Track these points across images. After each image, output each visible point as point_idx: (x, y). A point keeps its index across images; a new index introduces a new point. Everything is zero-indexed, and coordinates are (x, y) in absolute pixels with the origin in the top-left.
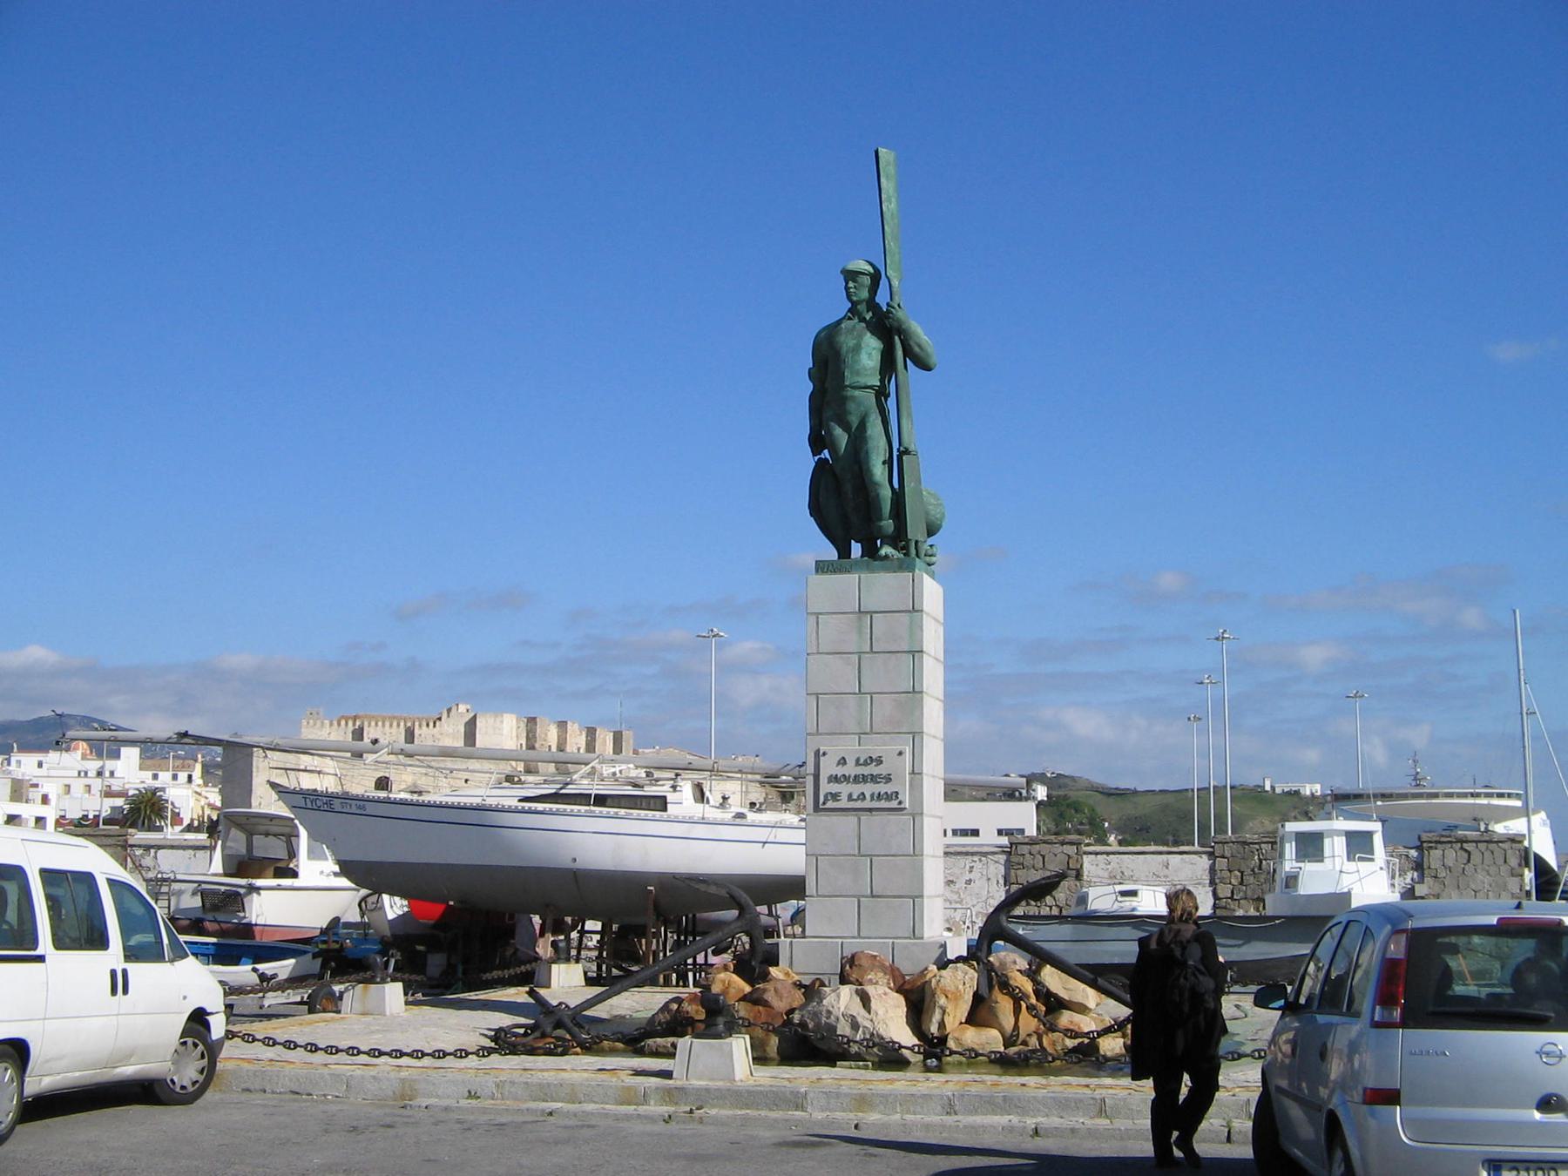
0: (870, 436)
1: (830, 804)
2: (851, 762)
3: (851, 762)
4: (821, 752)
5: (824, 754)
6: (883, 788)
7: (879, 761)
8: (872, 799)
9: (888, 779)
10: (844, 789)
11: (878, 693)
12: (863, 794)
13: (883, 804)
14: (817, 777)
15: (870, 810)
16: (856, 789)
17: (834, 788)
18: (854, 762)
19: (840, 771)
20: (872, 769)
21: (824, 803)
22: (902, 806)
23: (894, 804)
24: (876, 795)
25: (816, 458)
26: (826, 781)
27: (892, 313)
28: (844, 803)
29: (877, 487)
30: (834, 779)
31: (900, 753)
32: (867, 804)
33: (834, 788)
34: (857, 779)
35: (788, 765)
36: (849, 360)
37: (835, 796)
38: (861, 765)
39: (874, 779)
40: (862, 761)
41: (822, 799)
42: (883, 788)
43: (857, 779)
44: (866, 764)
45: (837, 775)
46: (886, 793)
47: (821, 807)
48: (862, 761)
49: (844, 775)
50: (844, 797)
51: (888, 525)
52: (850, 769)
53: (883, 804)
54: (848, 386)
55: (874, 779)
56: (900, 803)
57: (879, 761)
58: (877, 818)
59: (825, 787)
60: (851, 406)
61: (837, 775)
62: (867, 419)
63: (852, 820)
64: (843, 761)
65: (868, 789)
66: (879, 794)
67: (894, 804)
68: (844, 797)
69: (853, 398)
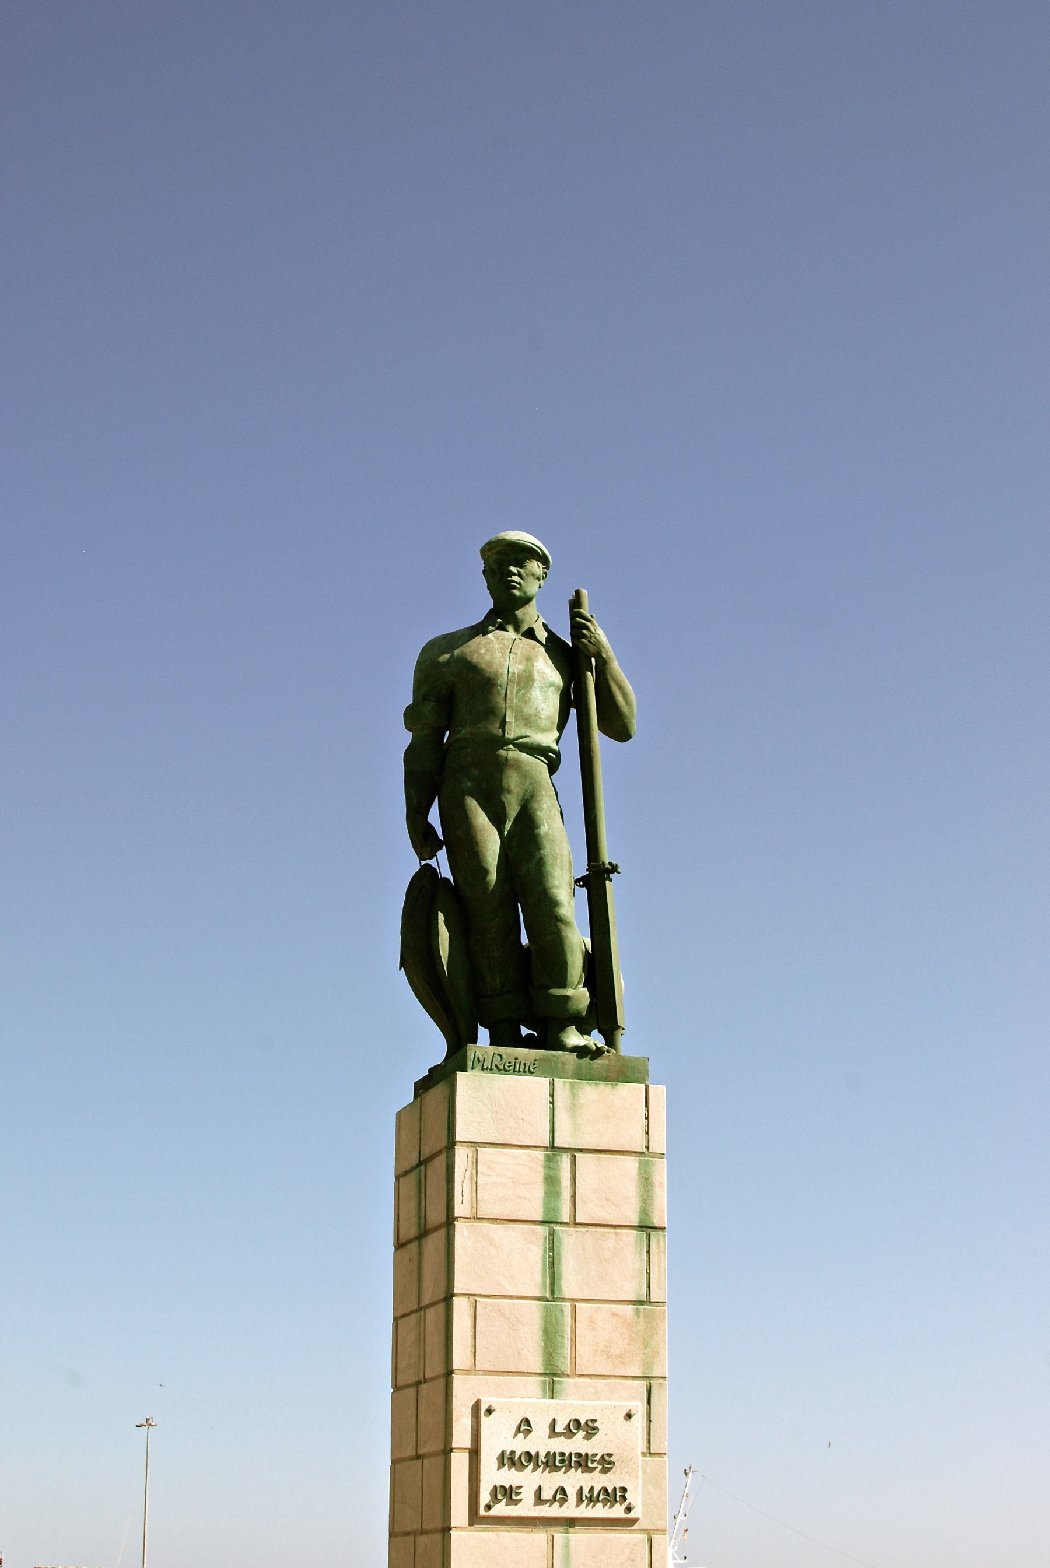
0: (547, 834)
1: (501, 1509)
2: (540, 1428)
3: (540, 1428)
4: (484, 1408)
5: (489, 1411)
6: (597, 1480)
7: (591, 1429)
8: (580, 1500)
9: (606, 1463)
10: (528, 1480)
11: (584, 1300)
12: (563, 1490)
13: (599, 1511)
14: (475, 1453)
15: (571, 1523)
16: (550, 1482)
17: (509, 1477)
18: (547, 1431)
19: (520, 1445)
20: (578, 1444)
21: (488, 1507)
22: (632, 1515)
23: (618, 1511)
24: (586, 1492)
25: (423, 863)
26: (495, 1463)
27: (587, 628)
28: (526, 1508)
29: (562, 927)
30: (508, 1460)
31: (629, 1416)
32: (570, 1510)
33: (509, 1477)
34: (552, 1462)
35: (685, 1470)
36: (513, 699)
37: (509, 1494)
38: (560, 1434)
39: (583, 1462)
40: (560, 1428)
41: (485, 1498)
42: (597, 1480)
43: (552, 1462)
44: (569, 1433)
45: (513, 1452)
46: (605, 1490)
47: (482, 1512)
48: (560, 1428)
49: (528, 1454)
50: (527, 1496)
51: (579, 995)
52: (540, 1443)
53: (599, 1511)
54: (511, 741)
55: (583, 1462)
56: (629, 1509)
57: (591, 1429)
58: (579, 1537)
59: (492, 1476)
60: (512, 781)
61: (513, 1452)
62: (535, 806)
63: (538, 1537)
64: (525, 1426)
65: (573, 1480)
66: (592, 1489)
67: (618, 1511)
68: (527, 1496)
69: (517, 765)
